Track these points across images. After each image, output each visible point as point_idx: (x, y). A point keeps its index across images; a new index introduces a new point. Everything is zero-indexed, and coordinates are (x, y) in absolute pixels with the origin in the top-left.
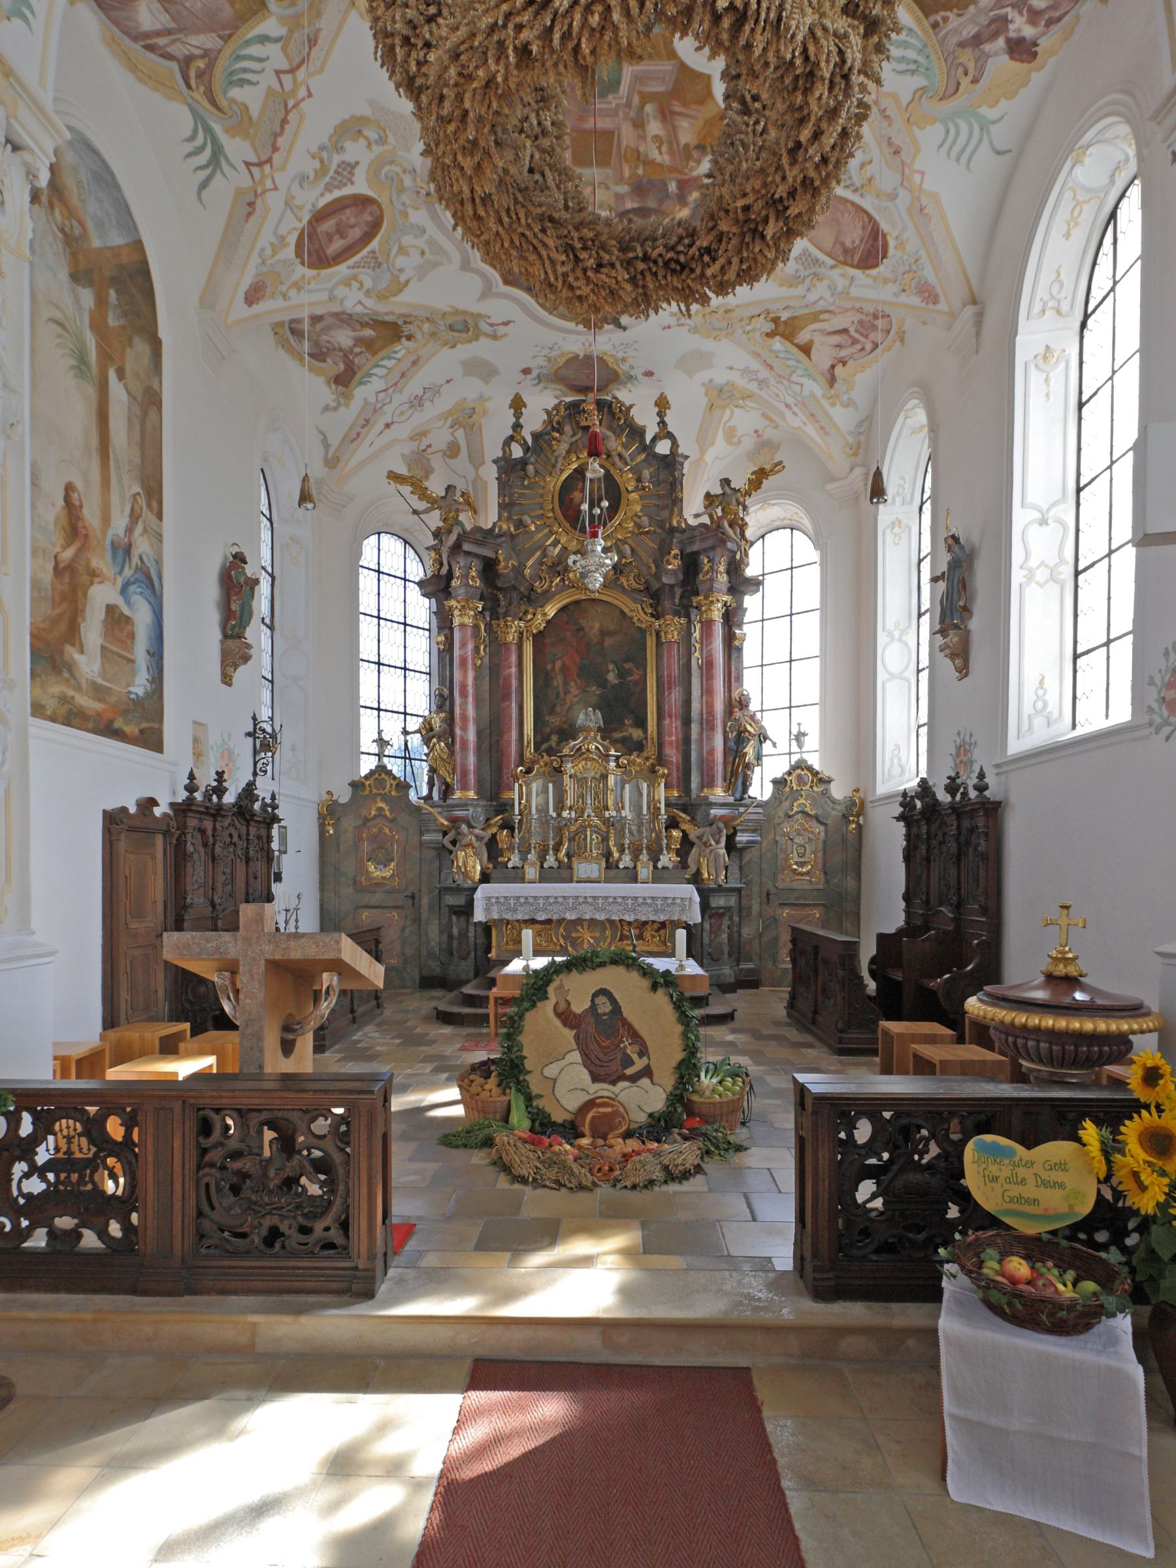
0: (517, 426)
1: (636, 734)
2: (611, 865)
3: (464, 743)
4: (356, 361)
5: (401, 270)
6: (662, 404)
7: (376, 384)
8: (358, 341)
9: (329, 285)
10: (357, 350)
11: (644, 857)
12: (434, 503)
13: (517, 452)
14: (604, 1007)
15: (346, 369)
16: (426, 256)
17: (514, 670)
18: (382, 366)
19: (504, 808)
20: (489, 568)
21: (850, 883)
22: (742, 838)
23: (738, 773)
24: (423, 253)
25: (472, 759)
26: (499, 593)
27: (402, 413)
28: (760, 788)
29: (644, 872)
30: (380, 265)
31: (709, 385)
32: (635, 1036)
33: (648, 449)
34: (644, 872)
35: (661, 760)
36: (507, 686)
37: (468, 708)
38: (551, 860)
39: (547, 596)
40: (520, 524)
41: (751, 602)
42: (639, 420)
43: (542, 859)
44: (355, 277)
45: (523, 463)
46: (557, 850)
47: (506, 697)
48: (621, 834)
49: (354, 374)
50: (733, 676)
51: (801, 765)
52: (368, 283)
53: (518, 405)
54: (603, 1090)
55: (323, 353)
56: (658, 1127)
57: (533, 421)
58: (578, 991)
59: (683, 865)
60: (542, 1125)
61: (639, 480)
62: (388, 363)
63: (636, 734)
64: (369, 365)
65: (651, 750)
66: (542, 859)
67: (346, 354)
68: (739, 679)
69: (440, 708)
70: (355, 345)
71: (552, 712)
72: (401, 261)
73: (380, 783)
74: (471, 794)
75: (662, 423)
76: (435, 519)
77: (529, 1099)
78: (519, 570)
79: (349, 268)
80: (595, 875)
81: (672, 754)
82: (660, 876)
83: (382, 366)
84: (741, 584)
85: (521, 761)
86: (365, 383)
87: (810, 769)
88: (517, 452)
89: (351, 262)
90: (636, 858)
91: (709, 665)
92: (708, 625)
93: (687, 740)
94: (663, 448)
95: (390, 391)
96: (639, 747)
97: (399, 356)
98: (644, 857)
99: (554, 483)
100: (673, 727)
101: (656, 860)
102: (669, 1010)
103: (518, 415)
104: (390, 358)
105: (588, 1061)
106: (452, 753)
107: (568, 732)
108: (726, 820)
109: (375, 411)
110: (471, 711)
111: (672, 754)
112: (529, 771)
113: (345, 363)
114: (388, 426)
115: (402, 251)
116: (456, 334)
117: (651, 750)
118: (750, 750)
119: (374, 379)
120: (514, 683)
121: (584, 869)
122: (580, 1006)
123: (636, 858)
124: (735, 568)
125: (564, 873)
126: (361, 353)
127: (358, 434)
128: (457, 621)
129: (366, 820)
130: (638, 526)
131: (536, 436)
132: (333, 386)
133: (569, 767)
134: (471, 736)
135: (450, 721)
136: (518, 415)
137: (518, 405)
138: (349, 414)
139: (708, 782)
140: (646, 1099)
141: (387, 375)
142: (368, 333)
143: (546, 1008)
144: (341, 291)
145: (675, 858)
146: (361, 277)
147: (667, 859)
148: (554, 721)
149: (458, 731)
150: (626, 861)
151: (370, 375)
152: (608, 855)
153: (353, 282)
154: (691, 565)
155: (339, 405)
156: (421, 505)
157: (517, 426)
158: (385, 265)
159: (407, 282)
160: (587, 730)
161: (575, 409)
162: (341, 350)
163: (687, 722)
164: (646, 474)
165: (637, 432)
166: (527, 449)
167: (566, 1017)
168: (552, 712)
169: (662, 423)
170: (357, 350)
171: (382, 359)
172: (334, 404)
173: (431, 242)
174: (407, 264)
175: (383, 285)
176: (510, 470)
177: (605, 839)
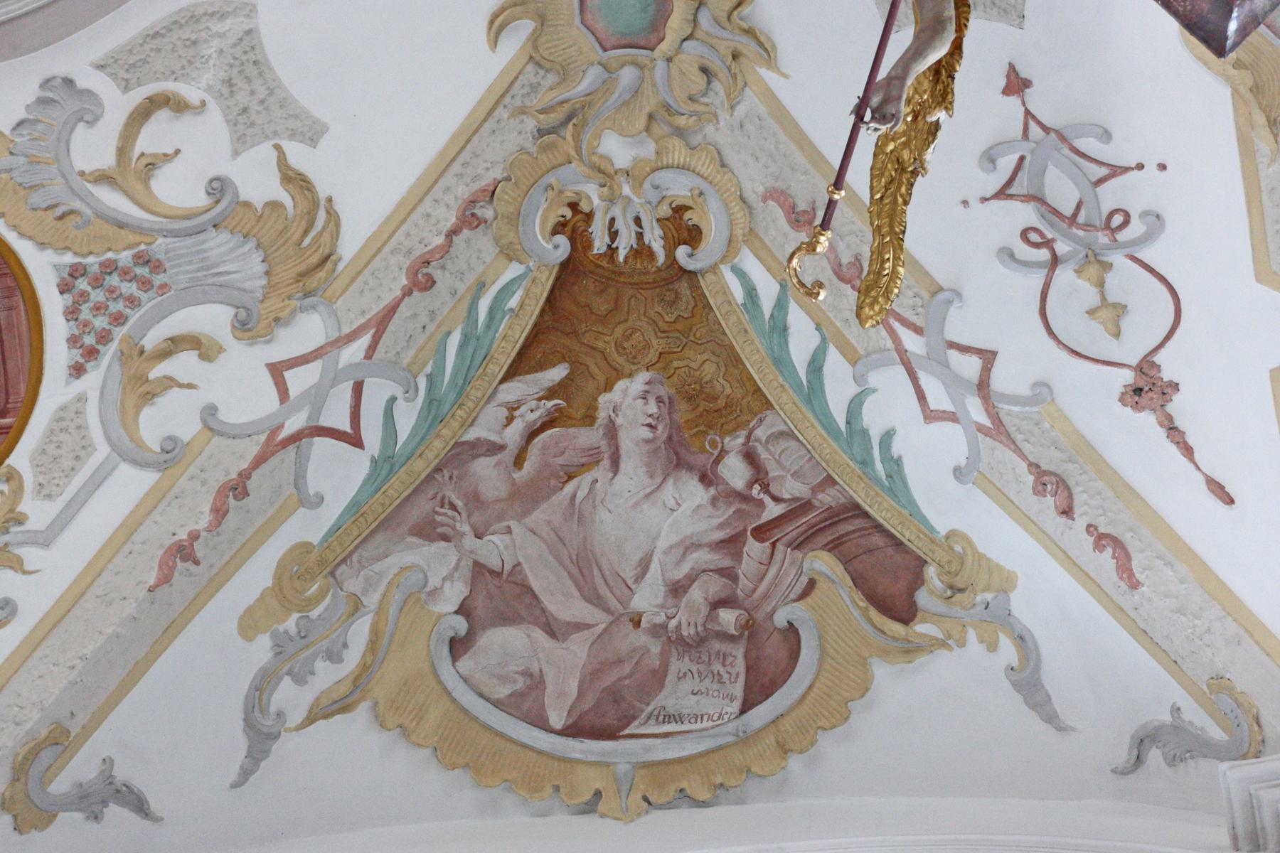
4: (792, 488)
5: (219, 187)
7: (890, 407)
8: (680, 452)
9: (102, 450)
10: (735, 472)
15: (834, 547)
16: (190, 92)
18: (816, 365)
24: (178, 105)
27: (1111, 314)
30: (143, 259)
44: (135, 354)
49: (857, 511)
52: (211, 319)
55: (751, 630)
62: (802, 339)
64: (812, 432)
67: (757, 524)
70: (706, 479)
72: (179, 188)
79: (77, 370)
83: (816, 365)
86: (895, 465)
89: (57, 354)
95: (912, 343)
97: (768, 290)
104: (780, 328)
109: (998, 429)
113: (800, 544)
114: (1148, 389)
115: (134, 170)
116: (676, 24)
119: (874, 420)
126: (750, 457)
127: (1102, 540)
132: (922, 628)
138: (1044, 583)
141: (853, 358)
142: (630, 401)
144: (165, 419)
146: (151, 340)
151: (855, 431)
153: (159, 370)
155: (1006, 621)
158: (160, 247)
159: (294, 179)
162: (732, 544)
170: (735, 472)
171: (782, 361)
172: (1008, 652)
173: (121, 66)
174: (197, 157)
175: (249, 269)
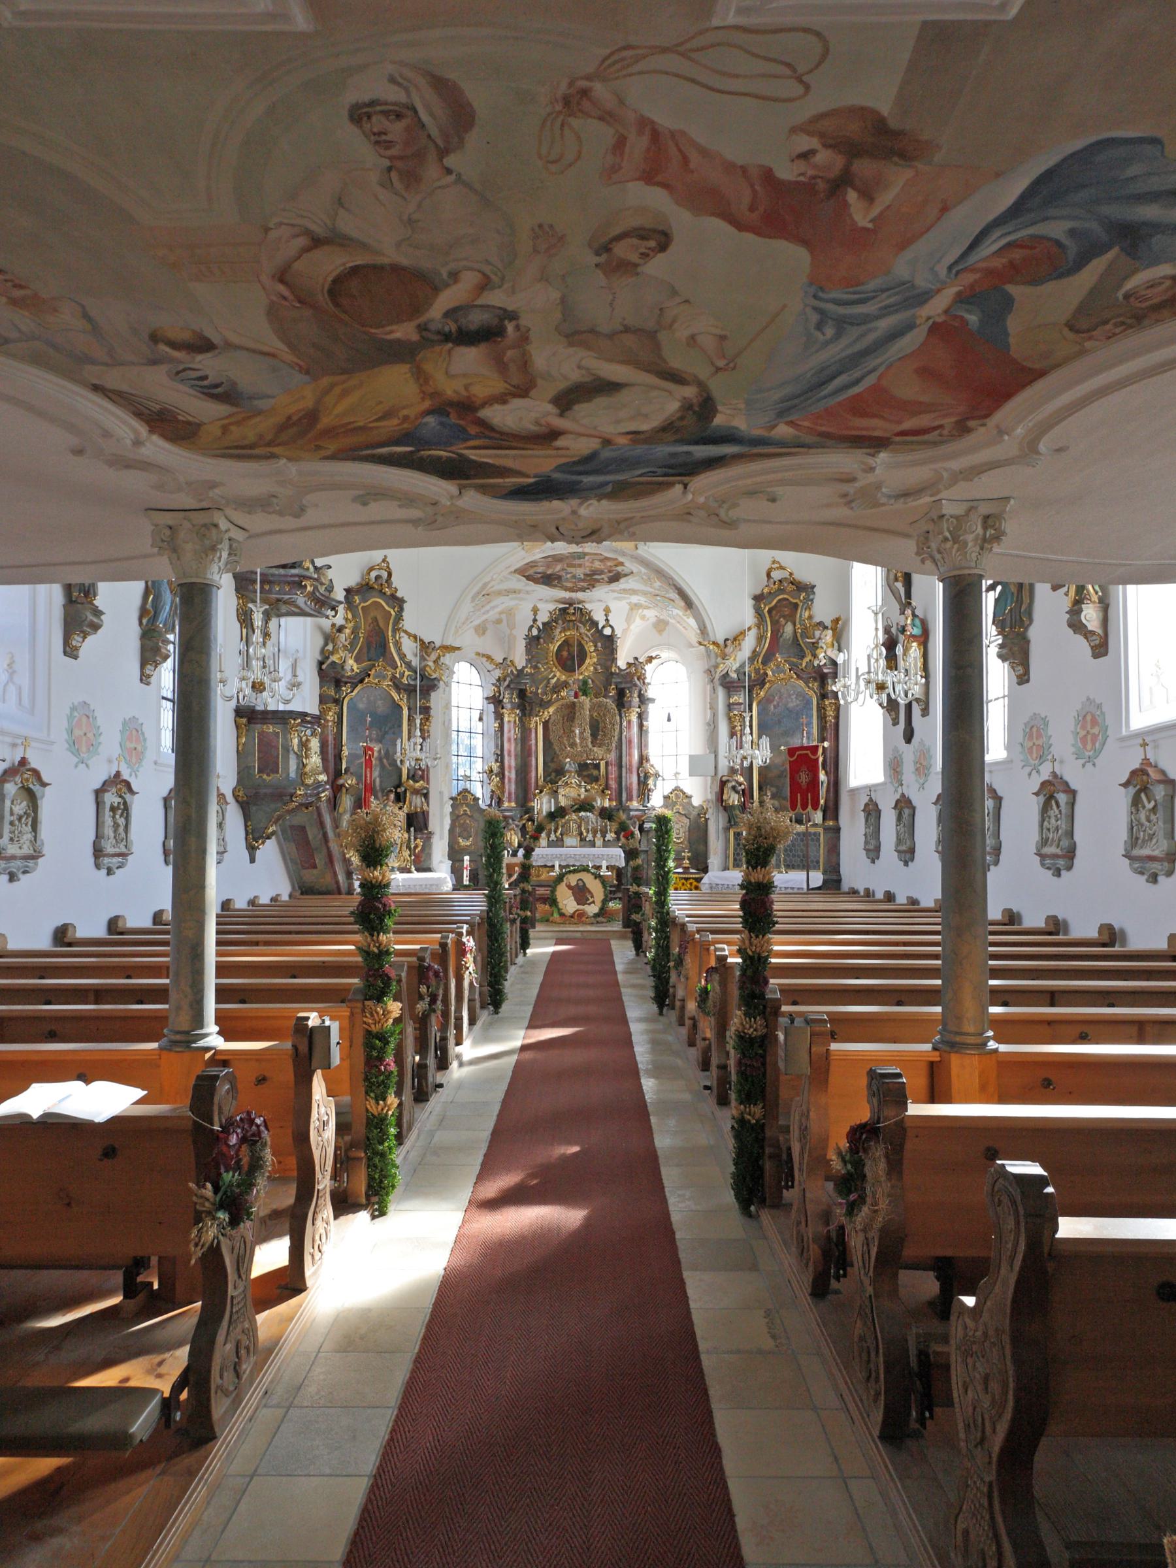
0: (535, 620)
1: (595, 772)
2: (583, 839)
3: (510, 779)
6: (607, 611)
11: (599, 835)
12: (498, 665)
13: (535, 632)
14: (581, 883)
17: (533, 742)
19: (529, 810)
20: (522, 694)
21: (702, 847)
22: (646, 825)
23: (644, 791)
25: (513, 787)
26: (526, 704)
28: (656, 801)
29: (599, 842)
31: (630, 604)
32: (590, 892)
33: (600, 632)
34: (599, 842)
35: (607, 787)
36: (530, 750)
37: (510, 762)
38: (553, 837)
39: (549, 703)
40: (536, 667)
41: (651, 707)
42: (596, 618)
43: (548, 836)
45: (538, 638)
46: (555, 832)
47: (530, 755)
48: (587, 823)
50: (642, 745)
51: (677, 789)
53: (535, 611)
54: (581, 907)
56: (596, 915)
57: (543, 617)
58: (573, 879)
59: (618, 839)
60: (562, 915)
61: (596, 646)
63: (595, 772)
65: (602, 781)
66: (548, 836)
68: (646, 746)
69: (497, 761)
71: (552, 761)
73: (465, 798)
74: (513, 804)
75: (607, 620)
76: (498, 673)
77: (559, 910)
78: (536, 694)
80: (574, 844)
81: (613, 784)
82: (606, 844)
84: (643, 700)
85: (537, 787)
87: (682, 791)
88: (535, 632)
90: (594, 836)
91: (630, 742)
92: (629, 722)
93: (620, 776)
94: (607, 631)
96: (596, 779)
98: (599, 835)
99: (554, 647)
100: (613, 770)
101: (604, 836)
102: (600, 885)
103: (535, 614)
105: (576, 899)
106: (503, 783)
107: (560, 772)
108: (638, 817)
110: (513, 764)
111: (613, 784)
112: (541, 792)
117: (602, 781)
118: (651, 782)
120: (533, 748)
121: (568, 841)
122: (573, 884)
123: (594, 836)
124: (640, 696)
125: (559, 843)
128: (506, 719)
129: (458, 816)
130: (595, 669)
131: (544, 624)
133: (561, 791)
134: (513, 776)
135: (502, 767)
136: (535, 614)
137: (535, 611)
139: (630, 799)
140: (592, 909)
143: (563, 884)
145: (613, 835)
147: (610, 836)
148: (553, 766)
149: (507, 773)
150: (590, 837)
152: (581, 834)
154: (621, 694)
156: (491, 667)
157: (535, 620)
160: (570, 772)
161: (563, 611)
163: (620, 767)
164: (599, 644)
165: (595, 624)
166: (539, 630)
167: (569, 887)
168: (552, 761)
169: (607, 620)
176: (533, 642)
177: (580, 826)
